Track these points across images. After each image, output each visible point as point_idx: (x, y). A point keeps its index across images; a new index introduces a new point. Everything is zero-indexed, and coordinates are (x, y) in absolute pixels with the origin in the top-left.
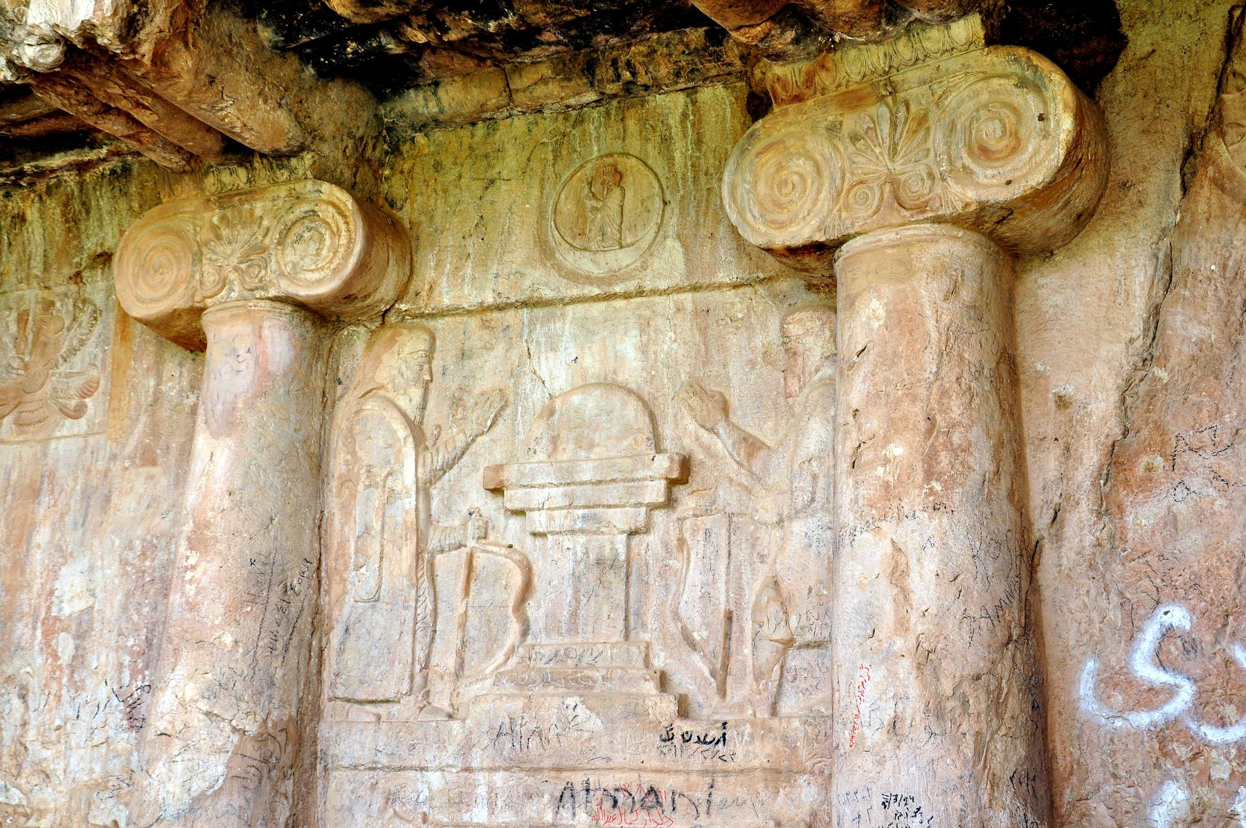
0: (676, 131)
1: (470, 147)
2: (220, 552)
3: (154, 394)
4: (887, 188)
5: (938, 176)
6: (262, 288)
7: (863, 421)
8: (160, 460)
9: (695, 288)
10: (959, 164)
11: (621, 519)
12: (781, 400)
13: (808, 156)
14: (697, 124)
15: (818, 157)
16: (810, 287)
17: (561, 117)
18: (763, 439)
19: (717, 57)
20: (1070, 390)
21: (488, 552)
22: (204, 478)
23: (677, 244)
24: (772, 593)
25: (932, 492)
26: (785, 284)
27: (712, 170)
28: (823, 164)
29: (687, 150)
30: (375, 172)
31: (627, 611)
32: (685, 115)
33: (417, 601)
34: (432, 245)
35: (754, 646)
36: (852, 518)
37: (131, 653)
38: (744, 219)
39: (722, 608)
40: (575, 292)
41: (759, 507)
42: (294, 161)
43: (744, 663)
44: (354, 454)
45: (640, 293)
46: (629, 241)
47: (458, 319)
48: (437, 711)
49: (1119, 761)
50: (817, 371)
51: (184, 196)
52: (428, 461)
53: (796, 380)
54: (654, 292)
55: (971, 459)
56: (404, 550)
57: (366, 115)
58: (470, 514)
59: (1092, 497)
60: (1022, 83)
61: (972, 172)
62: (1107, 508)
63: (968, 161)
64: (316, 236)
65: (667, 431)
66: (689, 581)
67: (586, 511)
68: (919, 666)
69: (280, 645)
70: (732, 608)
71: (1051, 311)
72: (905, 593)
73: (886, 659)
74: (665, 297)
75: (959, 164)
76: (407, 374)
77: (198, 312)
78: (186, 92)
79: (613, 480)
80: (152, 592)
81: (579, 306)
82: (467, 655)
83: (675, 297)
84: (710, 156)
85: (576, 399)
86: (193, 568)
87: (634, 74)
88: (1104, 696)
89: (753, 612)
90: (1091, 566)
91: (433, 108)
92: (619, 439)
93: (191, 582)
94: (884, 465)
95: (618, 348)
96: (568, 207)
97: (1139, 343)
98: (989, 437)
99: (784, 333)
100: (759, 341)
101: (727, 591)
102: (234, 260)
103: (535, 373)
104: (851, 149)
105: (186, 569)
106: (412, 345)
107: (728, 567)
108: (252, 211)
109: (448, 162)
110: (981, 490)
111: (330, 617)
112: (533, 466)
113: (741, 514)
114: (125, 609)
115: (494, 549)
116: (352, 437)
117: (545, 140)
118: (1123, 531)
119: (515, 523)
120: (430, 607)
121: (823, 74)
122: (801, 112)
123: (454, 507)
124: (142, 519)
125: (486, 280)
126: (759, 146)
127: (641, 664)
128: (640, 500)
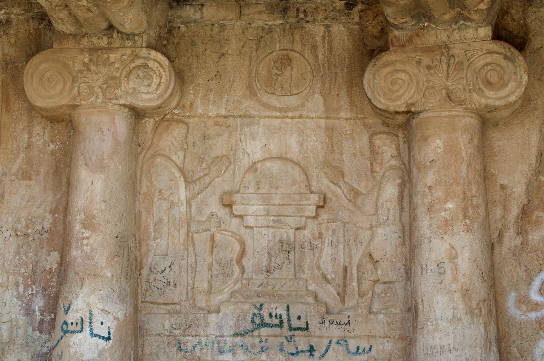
0: (319, 43)
1: (211, 36)
2: (102, 231)
3: (28, 142)
4: (444, 91)
5: (468, 90)
6: (116, 99)
7: (433, 191)
8: (34, 177)
9: (327, 118)
10: (477, 87)
12: (369, 173)
14: (330, 42)
15: (411, 73)
16: (384, 124)
17: (260, 29)
19: (348, 15)
20: (505, 182)
21: (222, 234)
22: (89, 193)
23: (320, 97)
24: (368, 259)
25: (466, 224)
26: (371, 121)
27: (337, 64)
29: (325, 53)
31: (295, 264)
32: (324, 37)
33: (188, 256)
35: (359, 283)
36: (429, 232)
37: (24, 277)
38: (374, 96)
39: (342, 265)
40: (268, 113)
42: (136, 38)
43: (353, 289)
44: (151, 182)
45: (300, 117)
46: (295, 92)
47: (202, 119)
48: (201, 309)
49: (523, 332)
50: (388, 162)
51: (67, 46)
52: (192, 189)
53: (378, 165)
54: (307, 117)
55: (479, 211)
56: (181, 231)
57: (165, 15)
58: (212, 215)
59: (515, 226)
60: (506, 57)
61: (483, 91)
62: (521, 231)
63: (482, 87)
64: (148, 76)
65: (314, 183)
66: (325, 252)
67: (275, 218)
68: (463, 296)
69: (128, 277)
70: (347, 264)
71: (497, 148)
72: (456, 267)
73: (448, 293)
74: (311, 120)
75: (477, 87)
77: (74, 107)
78: (119, 8)
79: (290, 204)
80: (33, 245)
81: (266, 119)
83: (316, 120)
84: (337, 58)
85: (268, 164)
86: (87, 238)
87: (306, 16)
88: (518, 306)
90: (514, 255)
91: (198, 16)
92: (293, 185)
93: (87, 245)
94: (445, 211)
95: (287, 141)
96: (263, 72)
97: (534, 165)
98: (484, 201)
99: (371, 143)
100: (357, 145)
101: (344, 258)
102: (99, 83)
104: (427, 72)
105: (83, 238)
106: (178, 131)
107: (344, 247)
108: (108, 58)
110: (483, 224)
111: (141, 263)
114: (17, 253)
115: (226, 233)
116: (150, 174)
117: (252, 38)
118: (527, 240)
119: (235, 221)
120: (194, 259)
121: (417, 38)
123: (203, 212)
124: (25, 208)
125: (221, 103)
126: (380, 63)
127: (304, 289)
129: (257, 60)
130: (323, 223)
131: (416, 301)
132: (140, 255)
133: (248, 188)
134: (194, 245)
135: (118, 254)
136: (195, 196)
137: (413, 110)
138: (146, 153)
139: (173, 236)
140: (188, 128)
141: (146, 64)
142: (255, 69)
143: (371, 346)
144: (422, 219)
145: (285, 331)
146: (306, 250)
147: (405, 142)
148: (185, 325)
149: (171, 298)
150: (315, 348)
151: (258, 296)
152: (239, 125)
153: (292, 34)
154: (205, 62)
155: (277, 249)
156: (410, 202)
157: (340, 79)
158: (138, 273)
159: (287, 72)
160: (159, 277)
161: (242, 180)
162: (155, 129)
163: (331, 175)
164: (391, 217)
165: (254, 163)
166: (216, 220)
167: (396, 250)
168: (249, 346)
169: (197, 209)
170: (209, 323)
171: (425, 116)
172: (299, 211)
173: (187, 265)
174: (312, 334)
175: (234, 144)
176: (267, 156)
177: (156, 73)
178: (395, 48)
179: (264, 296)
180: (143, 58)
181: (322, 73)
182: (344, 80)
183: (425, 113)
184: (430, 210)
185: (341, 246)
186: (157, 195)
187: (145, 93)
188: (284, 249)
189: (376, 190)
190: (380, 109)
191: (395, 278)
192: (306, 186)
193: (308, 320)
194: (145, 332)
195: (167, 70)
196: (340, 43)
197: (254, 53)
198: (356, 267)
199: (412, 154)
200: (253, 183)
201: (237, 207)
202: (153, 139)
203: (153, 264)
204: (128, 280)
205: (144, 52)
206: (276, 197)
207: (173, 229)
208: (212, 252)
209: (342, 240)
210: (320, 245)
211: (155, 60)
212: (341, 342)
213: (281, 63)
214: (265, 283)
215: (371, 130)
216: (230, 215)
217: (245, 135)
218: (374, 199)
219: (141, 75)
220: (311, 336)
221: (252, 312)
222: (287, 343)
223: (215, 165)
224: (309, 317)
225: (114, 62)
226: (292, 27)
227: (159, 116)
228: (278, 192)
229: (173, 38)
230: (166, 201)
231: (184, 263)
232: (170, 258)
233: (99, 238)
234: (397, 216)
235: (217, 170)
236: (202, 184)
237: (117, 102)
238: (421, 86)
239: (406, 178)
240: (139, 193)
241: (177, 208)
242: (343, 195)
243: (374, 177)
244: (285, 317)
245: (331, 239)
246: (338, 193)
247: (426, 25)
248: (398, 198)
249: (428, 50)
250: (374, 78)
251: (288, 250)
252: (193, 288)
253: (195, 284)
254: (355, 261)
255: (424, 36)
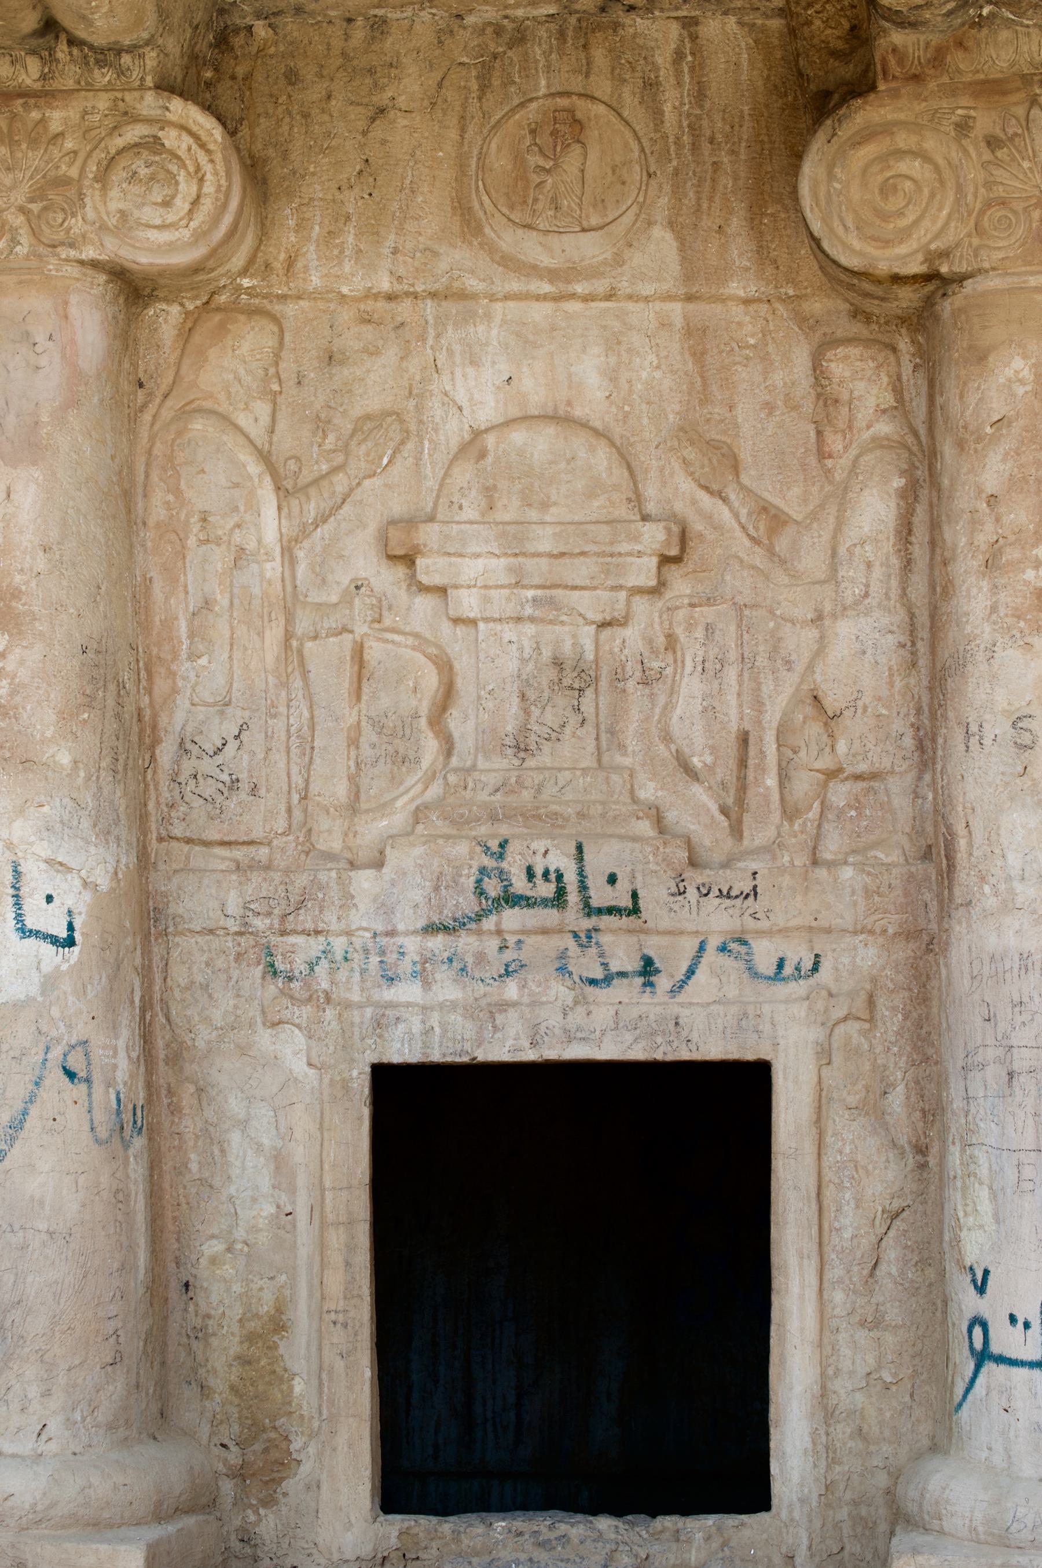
2: (42, 634)
6: (72, 246)
7: (1003, 509)
9: (690, 298)
11: (589, 604)
12: (812, 460)
13: (926, 158)
15: (941, 161)
16: (856, 313)
17: (489, 30)
18: (786, 509)
21: (387, 641)
23: (668, 236)
24: (809, 710)
26: (818, 305)
27: (719, 137)
28: (947, 174)
29: (683, 104)
30: (199, 73)
32: (679, 56)
33: (288, 707)
34: (290, 194)
35: (784, 778)
38: (832, 230)
40: (515, 285)
41: (781, 598)
42: (126, 59)
44: (177, 492)
45: (609, 297)
46: (594, 221)
47: (321, 305)
48: (329, 856)
50: (869, 427)
52: (296, 510)
53: (839, 436)
54: (630, 297)
56: (268, 634)
58: (357, 588)
64: (162, 176)
65: (651, 491)
66: (684, 691)
67: (539, 592)
69: (120, 768)
70: (747, 726)
76: (248, 379)
79: (583, 554)
81: (511, 304)
82: (364, 782)
83: (658, 305)
84: (717, 117)
85: (518, 436)
89: (781, 733)
92: (591, 494)
95: (573, 369)
96: (500, 162)
100: (778, 378)
101: (741, 706)
102: (19, 197)
103: (446, 395)
104: (987, 156)
106: (252, 341)
107: (741, 675)
108: (43, 121)
109: (308, 72)
111: (154, 727)
112: (463, 526)
113: (755, 606)
115: (397, 638)
116: (173, 468)
117: (465, 60)
119: (424, 604)
120: (306, 714)
121: (960, 54)
122: (918, 97)
123: (330, 577)
125: (379, 255)
127: (626, 798)
128: (622, 582)
129: (483, 125)
130: (677, 608)
131: (949, 827)
132: (151, 704)
133: (461, 508)
134: (305, 674)
135: (89, 702)
136: (305, 532)
137: (944, 269)
138: (160, 406)
139: (245, 649)
140: (282, 331)
141: (155, 137)
142: (475, 152)
143: (817, 956)
144: (968, 590)
145: (573, 916)
146: (631, 684)
147: (916, 367)
148: (284, 902)
149: (243, 828)
150: (658, 964)
151: (494, 818)
152: (431, 321)
153: (585, 46)
154: (328, 134)
155: (545, 682)
156: (933, 544)
157: (726, 182)
158: (147, 757)
159: (571, 161)
160: (207, 766)
161: (441, 485)
162: (186, 333)
163: (702, 467)
164: (876, 588)
165: (477, 434)
166: (368, 601)
167: (891, 684)
168: (470, 960)
169: (313, 571)
170: (353, 897)
171: (980, 288)
172: (608, 573)
173: (288, 731)
174: (650, 924)
175: (418, 378)
176: (514, 412)
177: (185, 166)
178: (894, 85)
179: (509, 818)
180: (148, 121)
181: (675, 163)
182: (741, 183)
183: (979, 278)
184: (991, 564)
185: (731, 674)
186: (195, 531)
187: (155, 227)
188: (567, 682)
189: (832, 509)
190: (846, 269)
191: (886, 764)
192: (629, 500)
193: (639, 886)
194: (170, 923)
195: (218, 157)
196: (726, 72)
197: (474, 106)
198: (774, 732)
199: (939, 400)
200: (474, 493)
201: (429, 561)
202: (179, 365)
203: (189, 729)
204: (119, 777)
205: (149, 103)
206: (541, 532)
207: (244, 628)
208: (358, 694)
209: (733, 655)
210: (669, 671)
211: (183, 128)
212: (733, 946)
213: (554, 133)
214: (513, 780)
215: (818, 334)
216: (409, 585)
217: (450, 352)
218: (826, 536)
219: (143, 172)
220: (646, 932)
221: (475, 865)
222: (579, 950)
223: (365, 440)
224: (639, 878)
225: (61, 135)
226: (584, 24)
227: (196, 297)
228: (548, 518)
229: (232, 62)
230: (224, 547)
231: (278, 725)
232: (239, 713)
233: (35, 655)
234: (894, 583)
235: (368, 454)
236: (326, 495)
237: (72, 253)
238: (970, 197)
239: (921, 473)
240: (144, 524)
241: (254, 567)
242: (736, 526)
243: (828, 473)
244: (571, 878)
245: (701, 653)
246: (721, 520)
247: (985, 12)
248: (898, 532)
249: (991, 89)
250: (831, 176)
251: (576, 686)
252: (305, 798)
253: (311, 786)
254: (772, 717)
255: (979, 45)
